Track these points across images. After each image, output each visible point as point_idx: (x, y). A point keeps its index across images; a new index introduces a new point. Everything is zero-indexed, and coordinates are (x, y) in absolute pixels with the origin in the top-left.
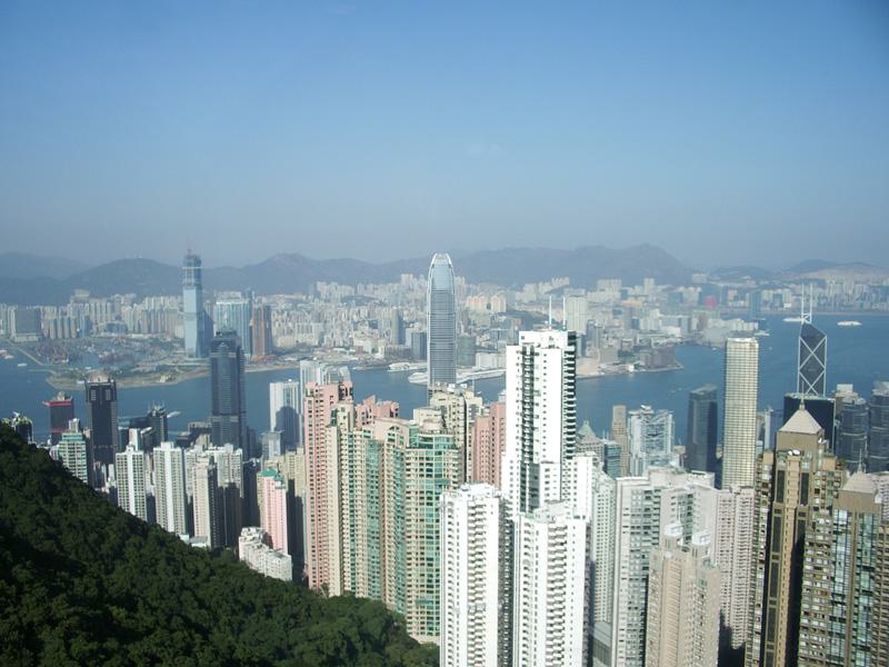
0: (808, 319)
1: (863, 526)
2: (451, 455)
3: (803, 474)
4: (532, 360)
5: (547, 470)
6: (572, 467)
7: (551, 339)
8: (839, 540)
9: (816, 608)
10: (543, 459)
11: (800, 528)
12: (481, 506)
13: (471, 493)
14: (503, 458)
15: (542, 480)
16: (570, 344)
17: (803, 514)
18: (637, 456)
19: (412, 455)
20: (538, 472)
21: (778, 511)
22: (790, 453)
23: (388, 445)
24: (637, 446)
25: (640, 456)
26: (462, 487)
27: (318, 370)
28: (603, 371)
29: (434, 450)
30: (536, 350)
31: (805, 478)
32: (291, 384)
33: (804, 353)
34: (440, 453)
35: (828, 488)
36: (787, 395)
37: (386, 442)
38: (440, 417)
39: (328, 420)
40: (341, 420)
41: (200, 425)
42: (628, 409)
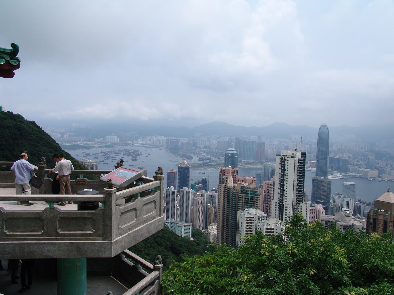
2: (256, 198)
4: (284, 162)
5: (286, 207)
6: (300, 207)
7: (293, 154)
12: (252, 218)
13: (250, 212)
14: (272, 200)
15: (284, 211)
19: (241, 197)
20: (283, 208)
22: (379, 210)
26: (246, 209)
29: (250, 195)
30: (286, 158)
34: (252, 197)
40: (225, 182)
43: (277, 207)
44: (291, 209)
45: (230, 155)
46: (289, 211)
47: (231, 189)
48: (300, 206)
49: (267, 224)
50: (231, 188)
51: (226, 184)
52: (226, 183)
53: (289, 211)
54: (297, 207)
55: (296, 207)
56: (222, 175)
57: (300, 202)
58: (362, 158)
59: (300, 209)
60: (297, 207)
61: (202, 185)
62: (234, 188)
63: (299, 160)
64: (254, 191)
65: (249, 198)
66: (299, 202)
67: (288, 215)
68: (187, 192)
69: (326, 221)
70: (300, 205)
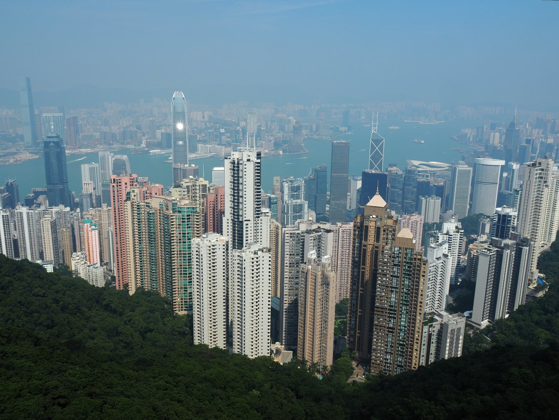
0: (375, 130)
1: (406, 254)
2: (195, 217)
3: (377, 227)
4: (238, 167)
5: (247, 224)
6: (259, 222)
8: (395, 261)
9: (383, 294)
10: (244, 219)
11: (375, 254)
12: (213, 246)
14: (223, 218)
15: (245, 230)
16: (258, 158)
17: (377, 247)
18: (286, 202)
19: (174, 217)
20: (242, 225)
21: (365, 246)
22: (371, 217)
23: (160, 210)
24: (286, 198)
25: (287, 202)
27: (110, 157)
28: (266, 153)
30: (241, 162)
31: (378, 230)
32: (94, 165)
33: (373, 148)
35: (389, 233)
36: (363, 171)
37: (159, 208)
38: (186, 193)
39: (124, 198)
40: (132, 197)
41: (40, 190)
42: (281, 179)
43: (230, 224)
44: (252, 225)
45: (52, 144)
46: (251, 229)
47: (143, 207)
48: (260, 220)
49: (250, 252)
50: (143, 205)
51: (134, 201)
52: (133, 199)
53: (251, 229)
54: (257, 222)
55: (255, 222)
56: (115, 186)
57: (259, 216)
58: (209, 132)
59: (260, 223)
60: (257, 222)
61: (10, 193)
62: (148, 205)
63: (255, 163)
64: (191, 207)
65: (186, 217)
66: (258, 216)
67: (249, 234)
68: (28, 213)
69: (291, 234)
70: (259, 219)
